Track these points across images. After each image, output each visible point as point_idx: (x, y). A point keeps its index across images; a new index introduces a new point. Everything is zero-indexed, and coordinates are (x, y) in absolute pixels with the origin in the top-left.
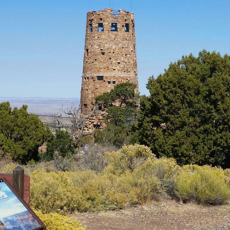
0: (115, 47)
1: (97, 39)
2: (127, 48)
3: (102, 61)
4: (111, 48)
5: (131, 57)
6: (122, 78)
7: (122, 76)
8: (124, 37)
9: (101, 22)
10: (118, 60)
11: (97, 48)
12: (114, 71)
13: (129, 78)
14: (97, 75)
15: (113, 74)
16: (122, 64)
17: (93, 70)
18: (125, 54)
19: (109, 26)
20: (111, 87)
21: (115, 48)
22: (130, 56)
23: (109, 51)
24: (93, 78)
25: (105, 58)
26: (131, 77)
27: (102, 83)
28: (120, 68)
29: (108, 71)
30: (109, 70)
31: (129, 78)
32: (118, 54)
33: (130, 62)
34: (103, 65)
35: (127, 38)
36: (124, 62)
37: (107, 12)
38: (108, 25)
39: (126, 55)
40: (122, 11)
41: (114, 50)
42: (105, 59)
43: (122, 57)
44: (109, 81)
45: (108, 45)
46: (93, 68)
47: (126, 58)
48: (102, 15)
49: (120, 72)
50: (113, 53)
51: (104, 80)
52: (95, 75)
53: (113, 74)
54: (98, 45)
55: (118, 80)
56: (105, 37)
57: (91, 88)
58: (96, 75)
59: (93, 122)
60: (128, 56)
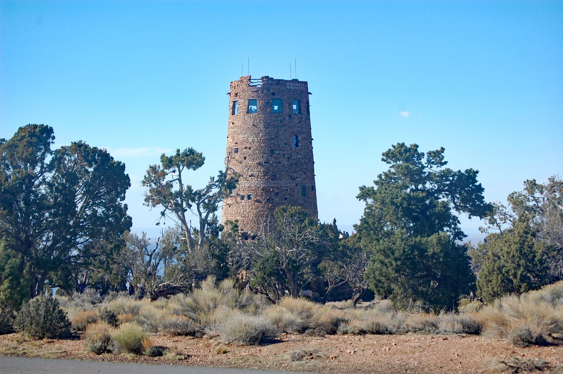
0: (252, 139)
2: (274, 139)
5: (284, 155)
12: (250, 178)
13: (277, 188)
26: (282, 187)
33: (279, 163)
45: (243, 136)
60: (277, 152)
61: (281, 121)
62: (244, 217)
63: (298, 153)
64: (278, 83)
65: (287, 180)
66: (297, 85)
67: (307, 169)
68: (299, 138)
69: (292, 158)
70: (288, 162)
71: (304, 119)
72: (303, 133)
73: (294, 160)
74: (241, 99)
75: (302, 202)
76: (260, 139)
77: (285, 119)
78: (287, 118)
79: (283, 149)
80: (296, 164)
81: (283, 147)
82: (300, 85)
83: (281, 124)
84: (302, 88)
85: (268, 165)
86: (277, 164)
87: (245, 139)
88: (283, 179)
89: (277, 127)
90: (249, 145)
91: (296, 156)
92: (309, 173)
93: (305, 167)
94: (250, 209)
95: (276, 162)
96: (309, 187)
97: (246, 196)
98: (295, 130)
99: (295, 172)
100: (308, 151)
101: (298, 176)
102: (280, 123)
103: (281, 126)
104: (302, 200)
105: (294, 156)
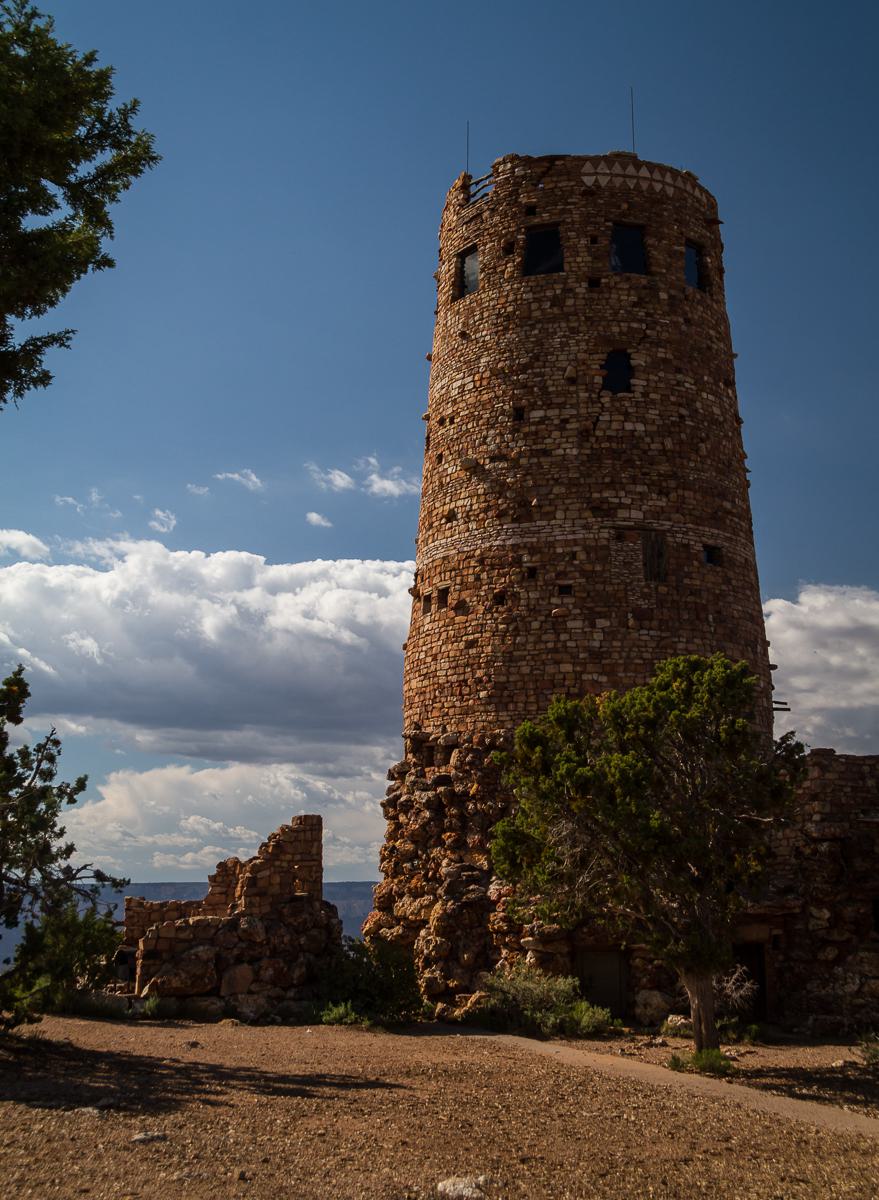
0: (459, 383)
5: (566, 421)
6: (481, 561)
8: (510, 309)
12: (449, 525)
13: (533, 550)
22: (551, 413)
26: (551, 545)
29: (430, 533)
32: (471, 417)
33: (546, 453)
35: (534, 306)
41: (455, 402)
49: (473, 525)
50: (452, 422)
60: (537, 414)
61: (556, 301)
63: (626, 415)
64: (549, 169)
65: (576, 515)
66: (631, 170)
67: (674, 476)
68: (639, 360)
69: (598, 433)
70: (580, 447)
71: (663, 296)
72: (658, 344)
73: (610, 439)
75: (644, 604)
76: (482, 379)
77: (571, 290)
78: (582, 289)
79: (561, 400)
80: (615, 454)
81: (558, 394)
82: (644, 172)
83: (556, 310)
84: (658, 187)
86: (535, 460)
87: (444, 391)
88: (560, 514)
89: (539, 321)
90: (450, 411)
91: (615, 426)
92: (687, 493)
93: (664, 468)
94: (440, 643)
95: (533, 453)
96: (687, 546)
97: (435, 595)
98: (616, 329)
99: (611, 485)
100: (684, 411)
101: (629, 501)
102: (551, 307)
103: (554, 319)
104: (644, 596)
105: (610, 424)
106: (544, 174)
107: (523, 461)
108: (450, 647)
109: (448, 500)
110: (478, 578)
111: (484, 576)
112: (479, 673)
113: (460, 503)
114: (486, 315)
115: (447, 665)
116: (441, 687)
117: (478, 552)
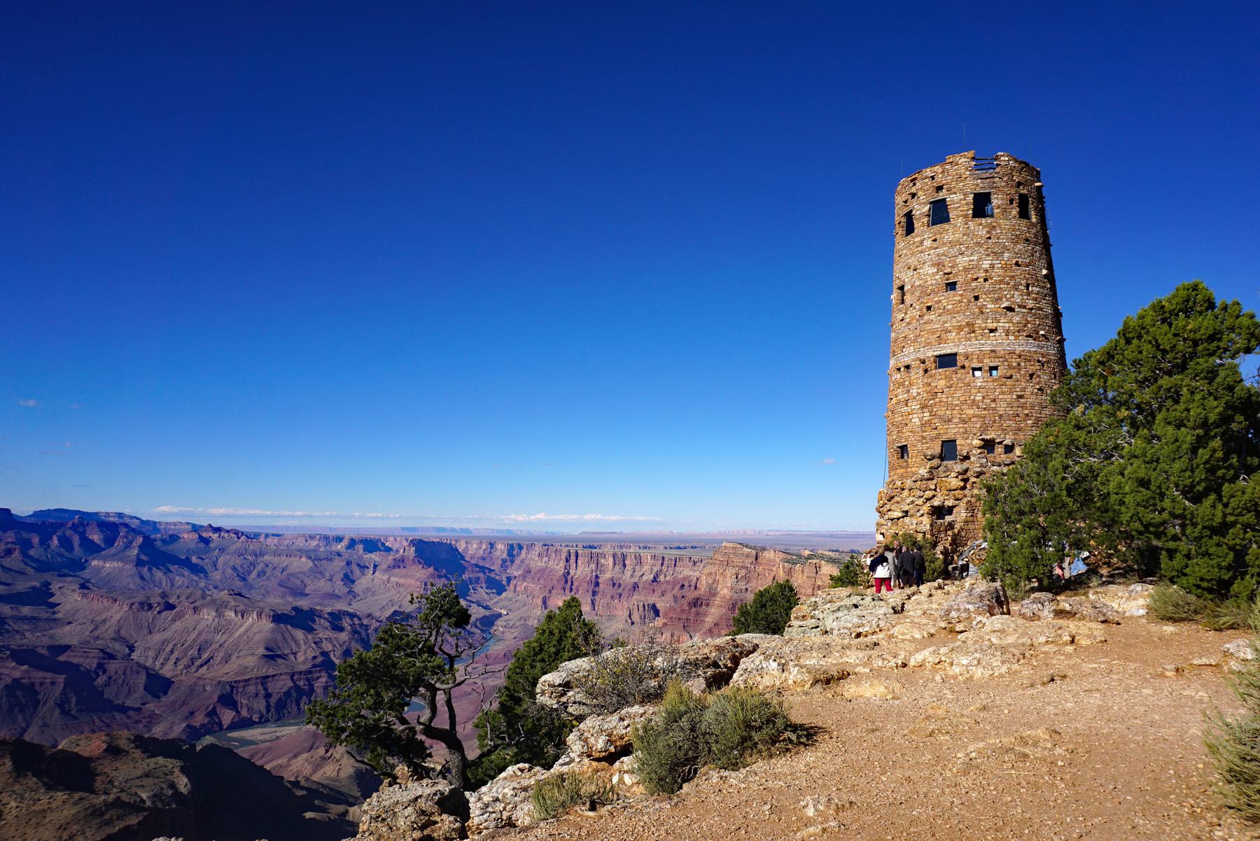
0: (990, 262)
1: (931, 248)
3: (950, 307)
4: (978, 267)
6: (1020, 356)
7: (1018, 349)
9: (941, 195)
10: (1004, 299)
11: (930, 272)
12: (992, 334)
13: (1043, 356)
14: (936, 354)
15: (988, 344)
16: (1018, 313)
17: (924, 339)
18: (1023, 282)
19: (967, 204)
20: (984, 384)
21: (992, 266)
23: (970, 276)
24: (923, 362)
25: (960, 298)
26: (1048, 354)
27: (954, 376)
28: (1011, 325)
29: (973, 335)
30: (974, 332)
31: (1043, 356)
32: (1001, 282)
34: (954, 320)
36: (1025, 307)
37: (957, 164)
38: (963, 202)
39: (1028, 286)
40: (1007, 159)
42: (960, 302)
43: (1016, 293)
44: (976, 365)
45: (968, 259)
46: (922, 333)
47: (1028, 294)
48: (940, 176)
49: (1011, 337)
50: (986, 280)
51: (959, 364)
52: (930, 354)
53: (988, 344)
54: (933, 265)
55: (1006, 363)
56: (957, 235)
57: (919, 394)
58: (931, 353)
59: (928, 500)
62: (985, 409)
74: (955, 193)
85: (1024, 310)
90: (984, 275)
106: (1022, 169)
107: (1033, 311)
108: (1006, 397)
109: (989, 321)
110: (1019, 365)
111: (1023, 364)
112: (1026, 412)
113: (1000, 324)
114: (1004, 232)
115: (1006, 405)
116: (1001, 416)
117: (1017, 352)
